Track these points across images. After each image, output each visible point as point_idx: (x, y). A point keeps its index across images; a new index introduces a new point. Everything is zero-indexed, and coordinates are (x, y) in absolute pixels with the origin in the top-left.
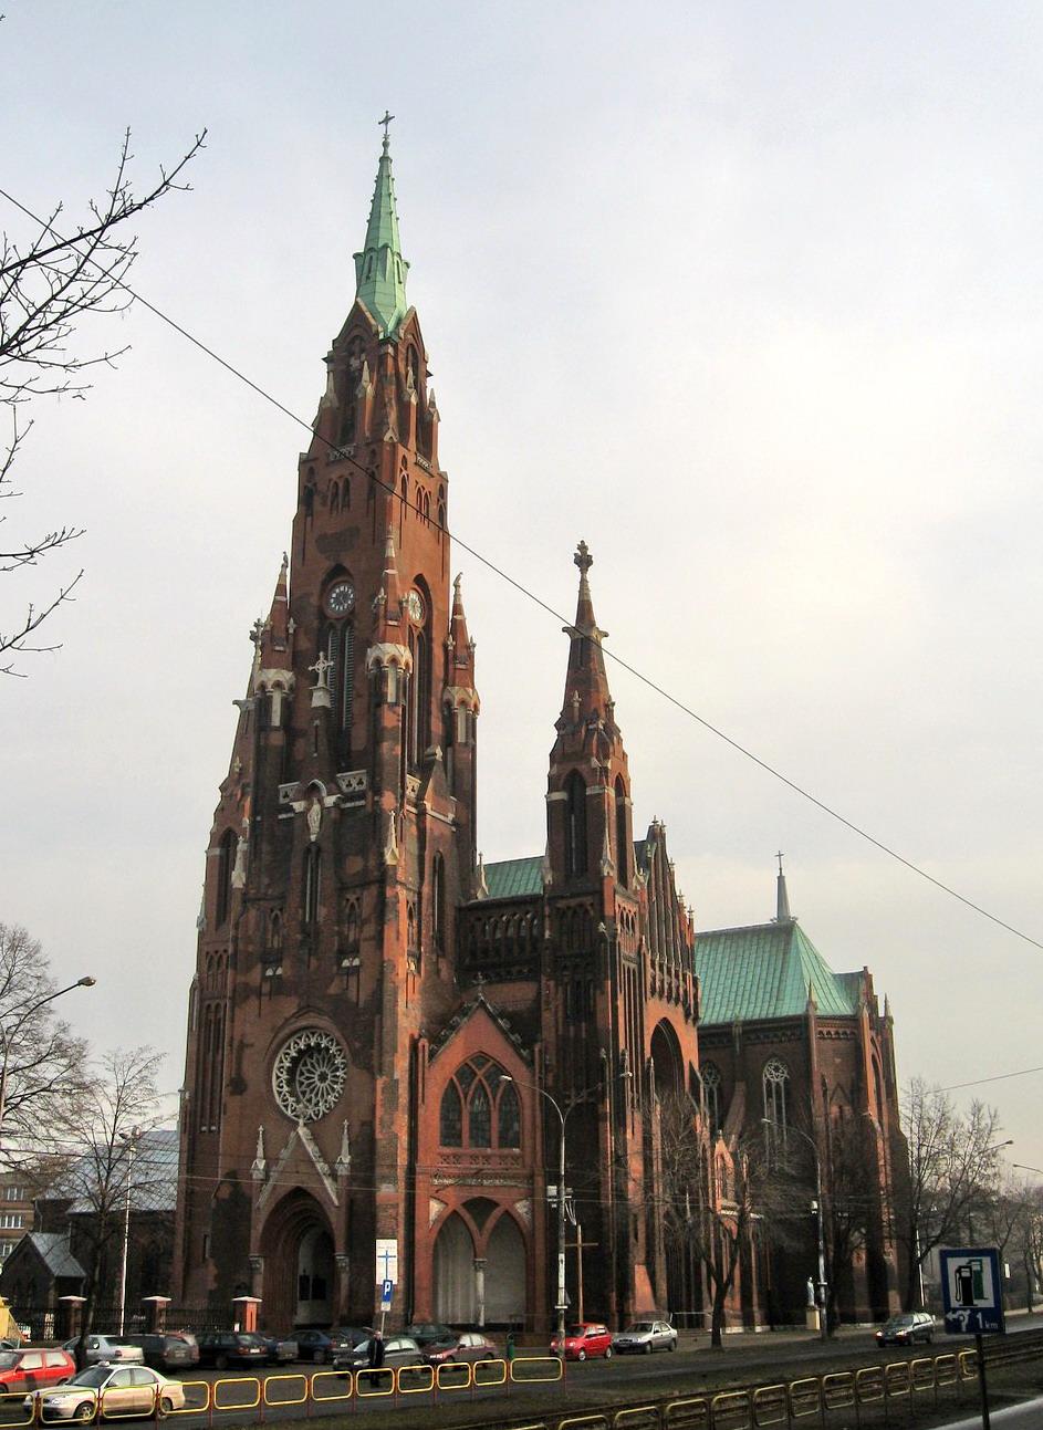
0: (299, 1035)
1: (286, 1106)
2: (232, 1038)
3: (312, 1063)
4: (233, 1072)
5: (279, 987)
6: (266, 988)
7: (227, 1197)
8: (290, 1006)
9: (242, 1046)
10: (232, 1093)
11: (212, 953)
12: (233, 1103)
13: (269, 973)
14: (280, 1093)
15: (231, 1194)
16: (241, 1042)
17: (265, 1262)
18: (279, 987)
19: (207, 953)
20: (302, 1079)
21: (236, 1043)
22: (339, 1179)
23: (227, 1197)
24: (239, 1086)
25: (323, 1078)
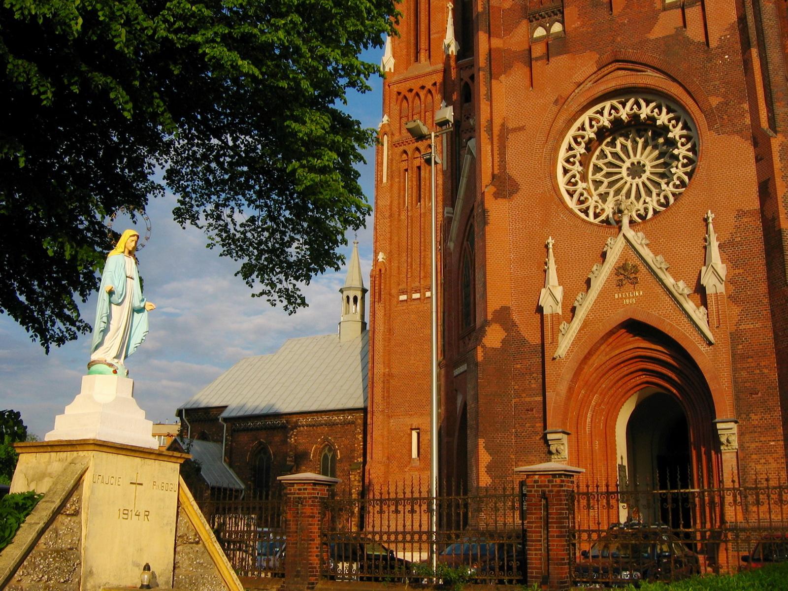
0: (598, 107)
1: (586, 212)
2: (491, 121)
3: (624, 147)
4: (496, 168)
5: (556, 47)
6: (538, 50)
7: (498, 345)
8: (583, 66)
9: (505, 132)
10: (497, 195)
11: (404, 92)
12: (498, 211)
13: (540, 32)
14: (571, 195)
15: (504, 341)
16: (503, 125)
17: (569, 441)
18: (556, 47)
19: (399, 93)
20: (599, 176)
21: (496, 130)
22: (711, 301)
23: (498, 345)
24: (505, 186)
25: (636, 170)
